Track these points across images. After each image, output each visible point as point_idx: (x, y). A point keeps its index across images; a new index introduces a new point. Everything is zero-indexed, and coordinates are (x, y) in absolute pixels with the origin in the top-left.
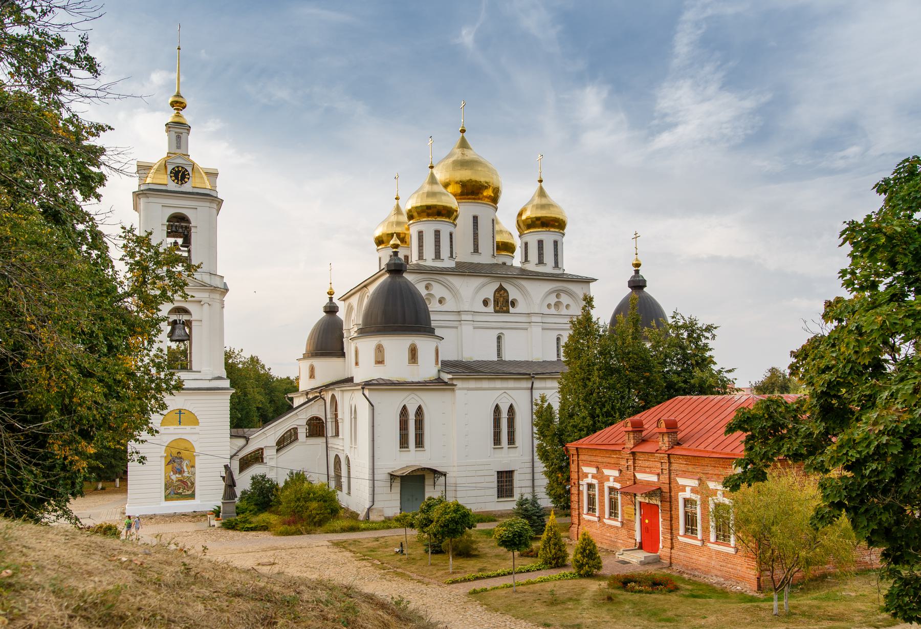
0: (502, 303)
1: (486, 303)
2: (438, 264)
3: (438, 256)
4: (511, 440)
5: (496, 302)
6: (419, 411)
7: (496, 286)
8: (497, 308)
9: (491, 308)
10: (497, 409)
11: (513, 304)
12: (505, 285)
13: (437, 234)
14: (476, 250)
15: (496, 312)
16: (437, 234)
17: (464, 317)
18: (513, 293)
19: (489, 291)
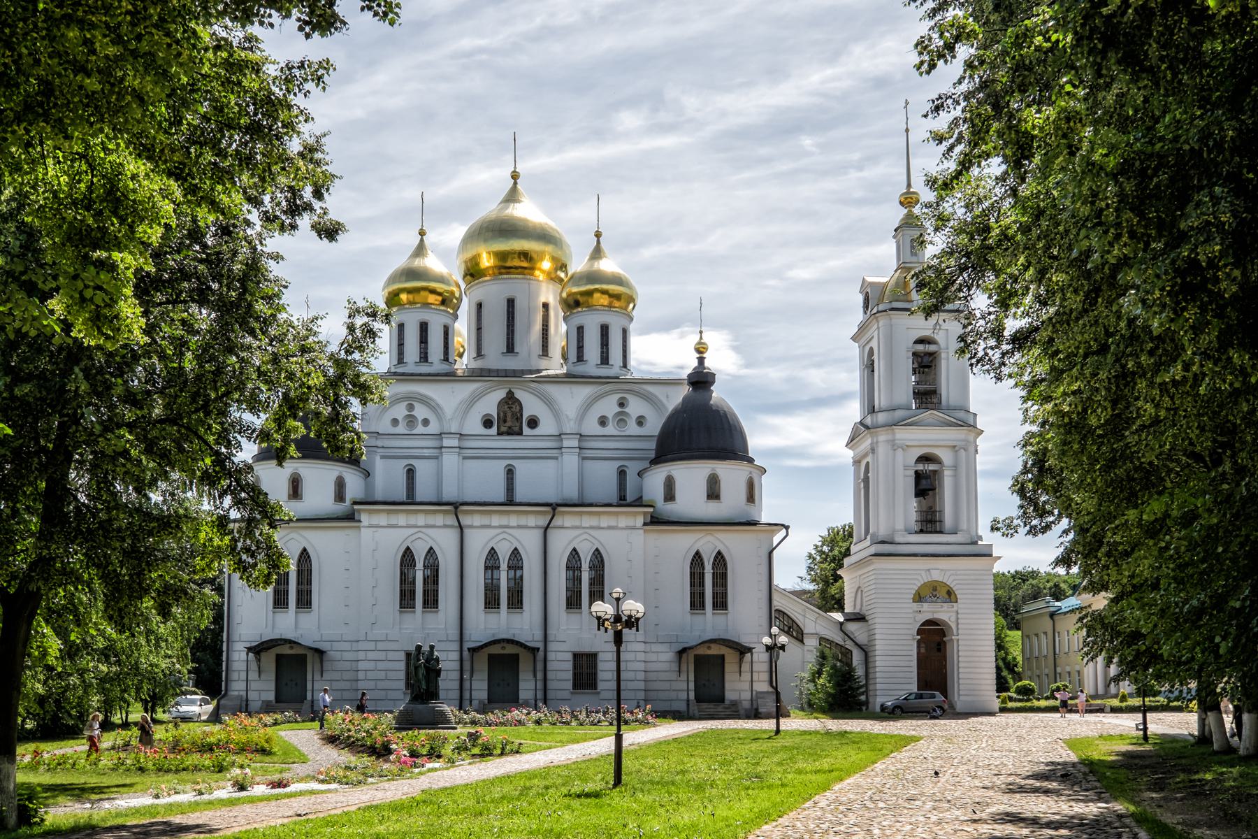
0: (510, 420)
1: (487, 423)
2: (424, 369)
3: (424, 357)
4: (431, 601)
5: (502, 419)
6: (304, 556)
7: (501, 394)
8: (503, 429)
9: (494, 430)
10: (408, 558)
11: (533, 423)
12: (519, 394)
13: (424, 327)
14: (510, 348)
15: (499, 434)
16: (424, 327)
17: (446, 442)
18: (531, 405)
19: (490, 403)
